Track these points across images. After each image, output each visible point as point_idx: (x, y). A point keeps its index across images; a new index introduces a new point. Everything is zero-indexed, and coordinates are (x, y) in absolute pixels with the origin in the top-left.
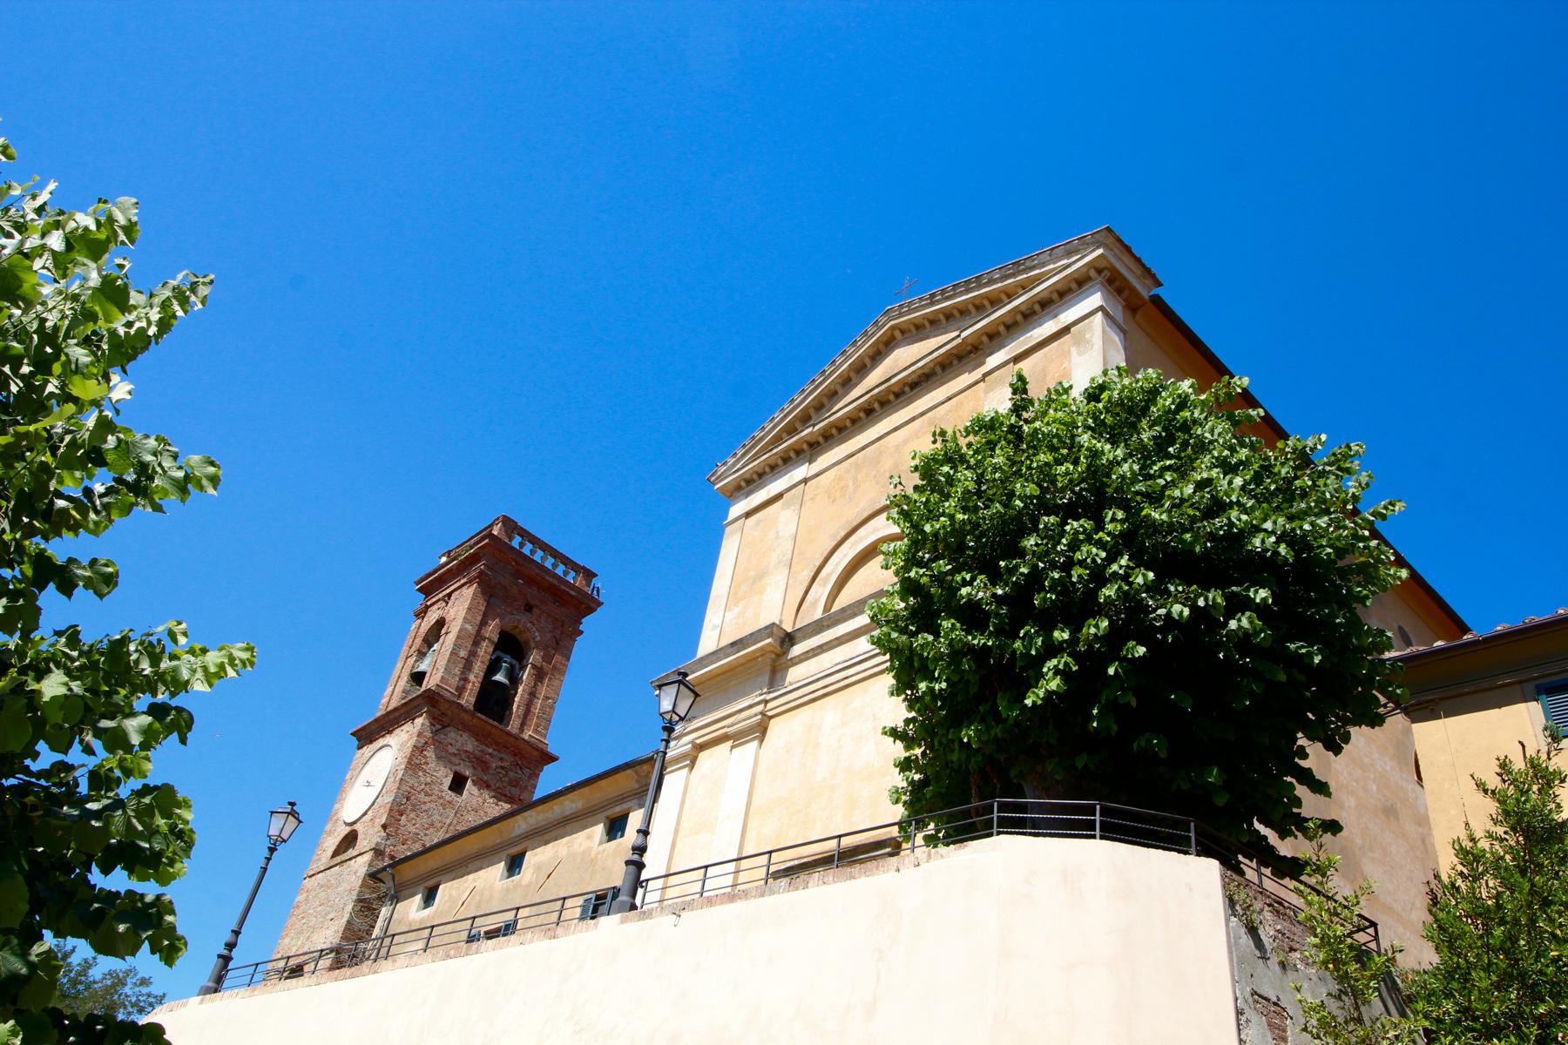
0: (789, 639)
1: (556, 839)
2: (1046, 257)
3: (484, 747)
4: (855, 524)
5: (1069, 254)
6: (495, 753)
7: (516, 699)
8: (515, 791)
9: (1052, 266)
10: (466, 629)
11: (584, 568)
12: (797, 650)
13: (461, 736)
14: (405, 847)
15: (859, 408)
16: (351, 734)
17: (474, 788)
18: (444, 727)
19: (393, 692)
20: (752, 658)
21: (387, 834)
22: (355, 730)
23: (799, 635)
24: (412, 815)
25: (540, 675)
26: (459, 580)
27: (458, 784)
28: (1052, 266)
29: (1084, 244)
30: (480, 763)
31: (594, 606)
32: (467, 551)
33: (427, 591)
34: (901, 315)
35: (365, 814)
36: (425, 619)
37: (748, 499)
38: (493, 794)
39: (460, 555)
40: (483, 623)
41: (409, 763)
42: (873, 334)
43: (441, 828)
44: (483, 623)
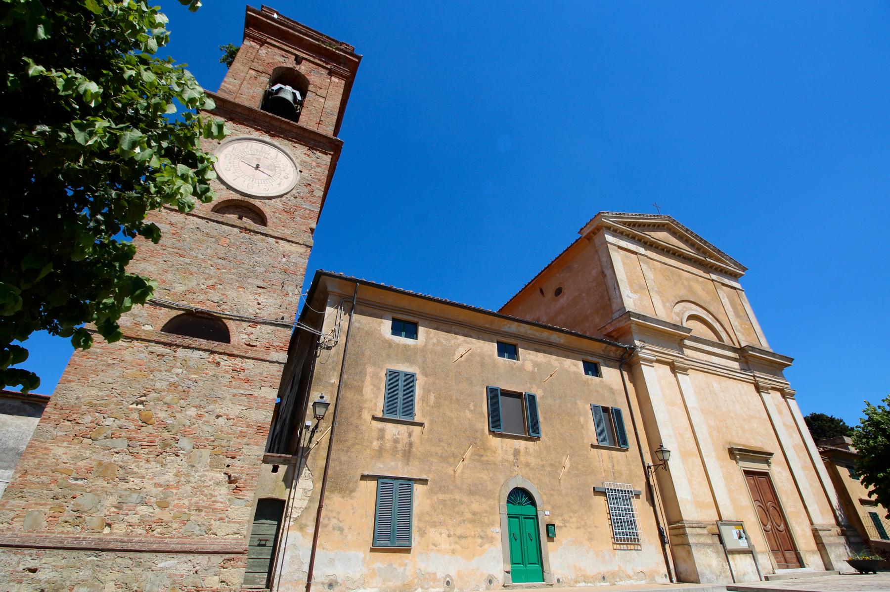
1: (544, 352)
2: (728, 258)
5: (735, 265)
15: (667, 247)
20: (674, 335)
34: (672, 223)
42: (663, 220)
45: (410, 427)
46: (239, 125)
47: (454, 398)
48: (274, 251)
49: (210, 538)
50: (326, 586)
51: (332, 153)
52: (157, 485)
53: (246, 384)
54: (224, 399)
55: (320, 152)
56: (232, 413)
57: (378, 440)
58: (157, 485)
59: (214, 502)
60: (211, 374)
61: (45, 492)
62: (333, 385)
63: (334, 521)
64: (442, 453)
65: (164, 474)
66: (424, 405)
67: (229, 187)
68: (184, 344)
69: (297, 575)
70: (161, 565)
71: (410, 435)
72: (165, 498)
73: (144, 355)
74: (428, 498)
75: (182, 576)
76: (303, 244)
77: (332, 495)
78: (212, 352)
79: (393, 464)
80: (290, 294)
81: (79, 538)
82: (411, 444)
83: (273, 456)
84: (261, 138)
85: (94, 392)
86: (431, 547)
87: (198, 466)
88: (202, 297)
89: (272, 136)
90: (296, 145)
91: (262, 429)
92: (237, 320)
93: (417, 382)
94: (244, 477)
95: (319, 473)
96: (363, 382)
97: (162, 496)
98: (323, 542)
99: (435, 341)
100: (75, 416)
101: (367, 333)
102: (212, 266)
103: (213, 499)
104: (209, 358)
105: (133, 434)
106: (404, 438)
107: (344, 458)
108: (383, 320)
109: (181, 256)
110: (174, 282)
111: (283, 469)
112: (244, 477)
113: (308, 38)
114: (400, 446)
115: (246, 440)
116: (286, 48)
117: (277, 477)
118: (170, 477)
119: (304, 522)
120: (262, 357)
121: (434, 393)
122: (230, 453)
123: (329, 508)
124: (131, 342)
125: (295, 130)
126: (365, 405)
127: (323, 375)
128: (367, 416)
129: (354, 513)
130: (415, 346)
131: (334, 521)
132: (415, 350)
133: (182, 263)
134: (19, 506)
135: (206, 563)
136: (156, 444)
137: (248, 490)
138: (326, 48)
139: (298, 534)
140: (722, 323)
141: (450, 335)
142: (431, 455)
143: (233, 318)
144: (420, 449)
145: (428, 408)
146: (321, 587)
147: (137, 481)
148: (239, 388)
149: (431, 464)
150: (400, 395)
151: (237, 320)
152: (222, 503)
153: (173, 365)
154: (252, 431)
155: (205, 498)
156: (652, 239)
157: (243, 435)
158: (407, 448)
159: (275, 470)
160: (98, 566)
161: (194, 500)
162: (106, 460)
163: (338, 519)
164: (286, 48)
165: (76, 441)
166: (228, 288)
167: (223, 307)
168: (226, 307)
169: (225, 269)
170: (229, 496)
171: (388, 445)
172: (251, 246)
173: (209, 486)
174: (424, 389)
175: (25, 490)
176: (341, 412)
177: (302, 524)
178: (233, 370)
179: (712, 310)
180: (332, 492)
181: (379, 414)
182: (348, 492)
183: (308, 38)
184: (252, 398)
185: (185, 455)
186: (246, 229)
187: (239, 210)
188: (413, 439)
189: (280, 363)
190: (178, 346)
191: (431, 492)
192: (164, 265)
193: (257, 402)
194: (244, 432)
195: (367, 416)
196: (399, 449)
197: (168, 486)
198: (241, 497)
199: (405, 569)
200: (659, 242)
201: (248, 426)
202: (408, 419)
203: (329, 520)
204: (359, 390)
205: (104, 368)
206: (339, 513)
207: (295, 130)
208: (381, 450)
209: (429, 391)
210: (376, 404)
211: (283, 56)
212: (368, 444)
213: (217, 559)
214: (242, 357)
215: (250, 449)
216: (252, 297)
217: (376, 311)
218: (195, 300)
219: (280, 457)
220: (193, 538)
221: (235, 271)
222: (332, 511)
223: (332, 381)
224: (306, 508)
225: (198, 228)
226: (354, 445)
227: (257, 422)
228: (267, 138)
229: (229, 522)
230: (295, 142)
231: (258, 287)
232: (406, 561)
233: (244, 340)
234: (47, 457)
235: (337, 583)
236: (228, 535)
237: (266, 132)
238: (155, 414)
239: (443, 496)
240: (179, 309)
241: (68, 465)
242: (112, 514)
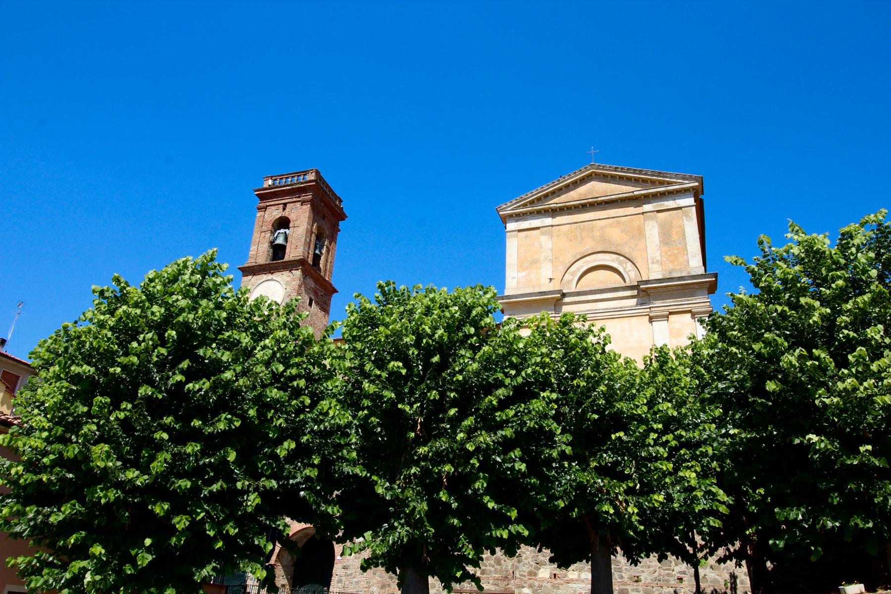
0: (564, 295)
4: (585, 254)
5: (684, 179)
7: (321, 262)
9: (675, 180)
11: (339, 198)
12: (566, 300)
15: (580, 204)
16: (239, 269)
18: (306, 276)
22: (241, 266)
23: (568, 295)
25: (328, 251)
27: (310, 304)
28: (675, 180)
29: (691, 178)
30: (316, 294)
34: (598, 169)
37: (517, 223)
40: (313, 225)
42: (584, 172)
55: (295, 270)
89: (272, 273)
90: (283, 273)
140: (635, 261)
156: (558, 205)
179: (626, 250)
200: (567, 204)
228: (270, 276)
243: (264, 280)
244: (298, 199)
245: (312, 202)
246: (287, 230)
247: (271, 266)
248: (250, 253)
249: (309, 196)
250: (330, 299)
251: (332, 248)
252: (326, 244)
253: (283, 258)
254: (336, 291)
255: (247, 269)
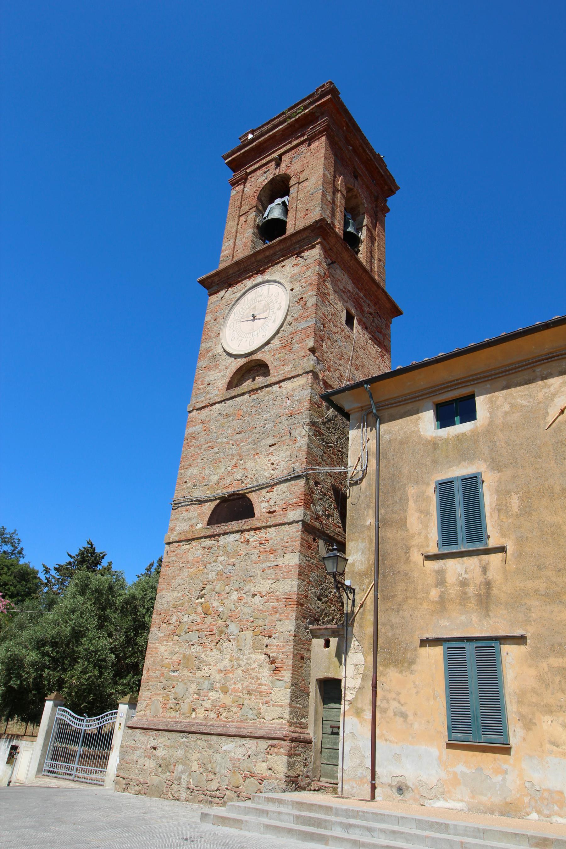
3: (357, 290)
6: (364, 298)
8: (381, 337)
10: (327, 176)
13: (344, 276)
14: (330, 374)
16: (202, 282)
17: (359, 326)
18: (333, 263)
19: (235, 245)
21: (317, 357)
24: (329, 343)
25: (372, 239)
26: (291, 142)
27: (349, 321)
31: (393, 188)
32: (303, 110)
33: (235, 166)
35: (268, 343)
36: (248, 185)
38: (370, 336)
39: (290, 117)
41: (318, 289)
43: (348, 359)
44: (335, 177)
45: (484, 557)
46: (236, 286)
47: (557, 488)
48: (279, 398)
49: (260, 722)
50: (395, 790)
51: (319, 240)
52: (220, 671)
53: (271, 555)
54: (256, 576)
56: (264, 590)
57: (437, 586)
58: (220, 671)
59: (260, 684)
60: (244, 554)
61: (159, 684)
62: (369, 528)
63: (394, 705)
64: (547, 588)
65: (222, 660)
66: (501, 517)
67: (236, 357)
68: (222, 532)
69: (360, 771)
70: (224, 748)
71: (485, 570)
72: (226, 683)
73: (200, 552)
74: (530, 666)
75: (239, 760)
76: (303, 373)
77: (388, 670)
78: (242, 532)
79: (463, 618)
80: (299, 439)
81: (178, 722)
82: (488, 584)
83: (320, 629)
84: (254, 283)
85: (175, 595)
86: (548, 746)
87: (244, 649)
88: (229, 480)
89: (262, 272)
90: (283, 264)
91: (290, 600)
92: (257, 490)
93: (485, 484)
94: (280, 656)
95: (368, 643)
96: (406, 511)
97: (223, 681)
98: (385, 732)
99: (506, 407)
100: (167, 618)
101: (402, 443)
102: (233, 445)
103: (259, 681)
104: (241, 538)
105: (201, 627)
106: (477, 577)
107: (395, 620)
108: (420, 415)
109: (212, 448)
110: (210, 475)
111: (334, 642)
112: (280, 656)
113: (277, 130)
114: (471, 590)
115: (277, 616)
116: (264, 161)
117: (329, 653)
118: (226, 663)
119: (359, 706)
120: (280, 522)
121: (516, 493)
122: (267, 632)
123: (386, 687)
124: (191, 543)
125: (278, 248)
126: (414, 542)
127: (357, 519)
128: (417, 557)
129: (417, 692)
130: (472, 431)
131: (394, 705)
132: (474, 436)
133: (213, 454)
134: (148, 697)
135: (255, 748)
136: (214, 632)
137: (285, 670)
138: (296, 120)
139: (355, 720)
141: (533, 385)
142: (527, 595)
143: (254, 489)
144: (504, 588)
145: (510, 521)
146: (388, 789)
147: (207, 668)
148: (266, 561)
149: (529, 609)
150: (460, 513)
151: (257, 490)
152: (265, 685)
153: (217, 555)
154: (281, 605)
155: (253, 682)
157: (275, 611)
158: (483, 591)
159: (327, 644)
160: (187, 746)
161: (246, 683)
162: (188, 652)
163: (399, 702)
164: (264, 161)
165: (170, 639)
166: (246, 461)
167: (245, 482)
168: (247, 481)
169: (242, 442)
170: (271, 678)
171: (453, 592)
172: (259, 405)
173: (254, 669)
174: (497, 491)
175: (149, 684)
176: (384, 560)
177: (359, 708)
178: (260, 544)
180: (386, 666)
181: (434, 549)
182: (406, 665)
183: (277, 130)
184: (277, 569)
185: (234, 639)
186: (253, 390)
187: (252, 372)
188: (490, 575)
189: (297, 522)
190: (219, 535)
191: (535, 655)
192: (202, 464)
193: (282, 571)
194: (276, 608)
195: (417, 557)
196: (470, 594)
197: (225, 672)
198: (280, 678)
199: (504, 779)
201: (278, 600)
202: (478, 546)
203: (388, 702)
204: (402, 523)
205: (178, 572)
206: (398, 694)
207: (278, 248)
208: (443, 601)
209: (508, 493)
210: (426, 537)
211: (265, 173)
212: (424, 595)
213: (263, 744)
214: (265, 527)
215: (283, 625)
216: (266, 459)
217: (409, 407)
218: (225, 486)
219: (326, 629)
220: (248, 723)
221: (250, 440)
222: (390, 691)
223: (368, 523)
224: (360, 688)
225: (220, 413)
226: (405, 600)
227: (284, 595)
228: (259, 278)
229: (273, 705)
230: (283, 261)
231: (270, 446)
232: (505, 767)
233: (265, 509)
234: (157, 655)
235: (408, 787)
236: (274, 719)
237: (257, 274)
238: (211, 604)
239: (560, 660)
240: (216, 499)
241: (168, 660)
242: (195, 700)
243: (247, 288)
244: (302, 139)
245: (328, 131)
246: (286, 199)
247: (260, 257)
248: (222, 254)
249: (323, 122)
250: (388, 326)
251: (379, 236)
252: (365, 222)
253: (285, 233)
254: (397, 312)
255: (216, 279)
